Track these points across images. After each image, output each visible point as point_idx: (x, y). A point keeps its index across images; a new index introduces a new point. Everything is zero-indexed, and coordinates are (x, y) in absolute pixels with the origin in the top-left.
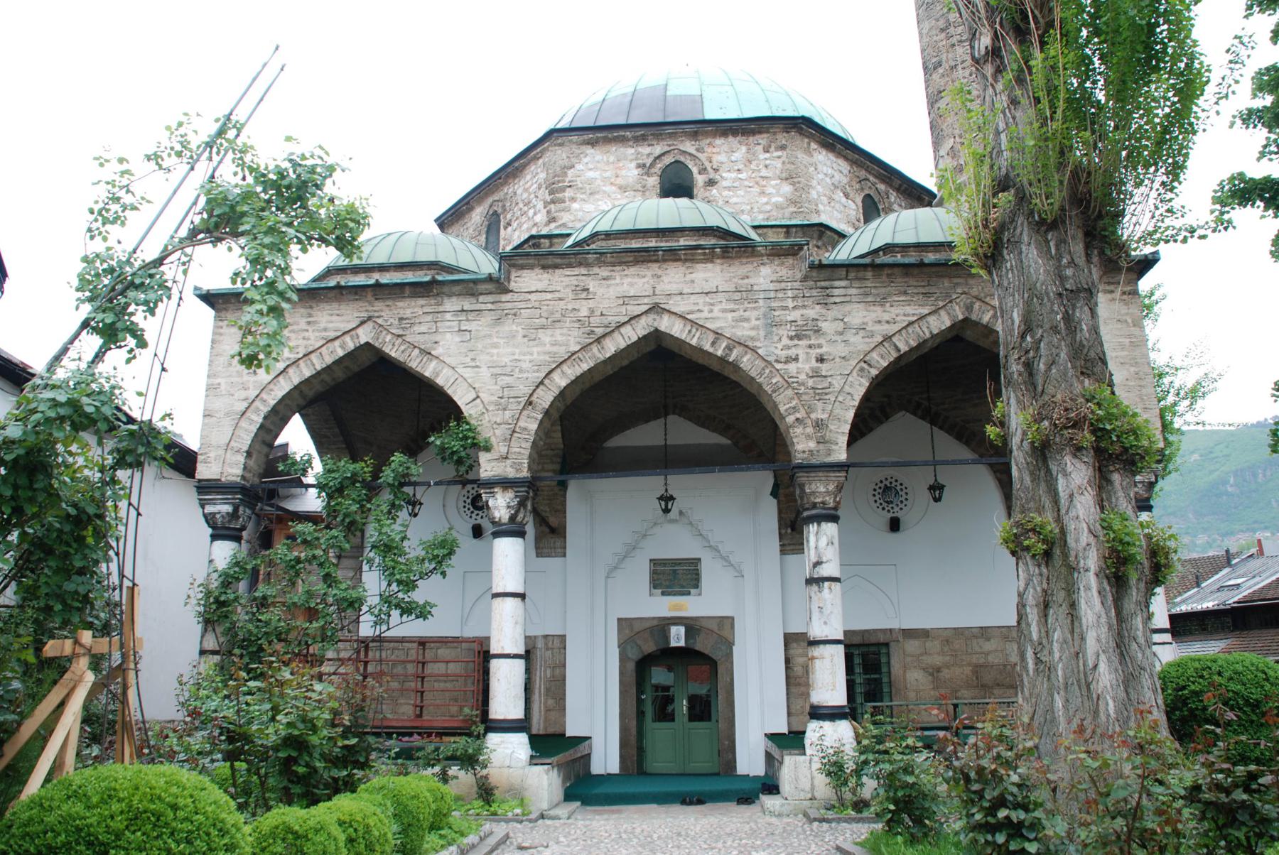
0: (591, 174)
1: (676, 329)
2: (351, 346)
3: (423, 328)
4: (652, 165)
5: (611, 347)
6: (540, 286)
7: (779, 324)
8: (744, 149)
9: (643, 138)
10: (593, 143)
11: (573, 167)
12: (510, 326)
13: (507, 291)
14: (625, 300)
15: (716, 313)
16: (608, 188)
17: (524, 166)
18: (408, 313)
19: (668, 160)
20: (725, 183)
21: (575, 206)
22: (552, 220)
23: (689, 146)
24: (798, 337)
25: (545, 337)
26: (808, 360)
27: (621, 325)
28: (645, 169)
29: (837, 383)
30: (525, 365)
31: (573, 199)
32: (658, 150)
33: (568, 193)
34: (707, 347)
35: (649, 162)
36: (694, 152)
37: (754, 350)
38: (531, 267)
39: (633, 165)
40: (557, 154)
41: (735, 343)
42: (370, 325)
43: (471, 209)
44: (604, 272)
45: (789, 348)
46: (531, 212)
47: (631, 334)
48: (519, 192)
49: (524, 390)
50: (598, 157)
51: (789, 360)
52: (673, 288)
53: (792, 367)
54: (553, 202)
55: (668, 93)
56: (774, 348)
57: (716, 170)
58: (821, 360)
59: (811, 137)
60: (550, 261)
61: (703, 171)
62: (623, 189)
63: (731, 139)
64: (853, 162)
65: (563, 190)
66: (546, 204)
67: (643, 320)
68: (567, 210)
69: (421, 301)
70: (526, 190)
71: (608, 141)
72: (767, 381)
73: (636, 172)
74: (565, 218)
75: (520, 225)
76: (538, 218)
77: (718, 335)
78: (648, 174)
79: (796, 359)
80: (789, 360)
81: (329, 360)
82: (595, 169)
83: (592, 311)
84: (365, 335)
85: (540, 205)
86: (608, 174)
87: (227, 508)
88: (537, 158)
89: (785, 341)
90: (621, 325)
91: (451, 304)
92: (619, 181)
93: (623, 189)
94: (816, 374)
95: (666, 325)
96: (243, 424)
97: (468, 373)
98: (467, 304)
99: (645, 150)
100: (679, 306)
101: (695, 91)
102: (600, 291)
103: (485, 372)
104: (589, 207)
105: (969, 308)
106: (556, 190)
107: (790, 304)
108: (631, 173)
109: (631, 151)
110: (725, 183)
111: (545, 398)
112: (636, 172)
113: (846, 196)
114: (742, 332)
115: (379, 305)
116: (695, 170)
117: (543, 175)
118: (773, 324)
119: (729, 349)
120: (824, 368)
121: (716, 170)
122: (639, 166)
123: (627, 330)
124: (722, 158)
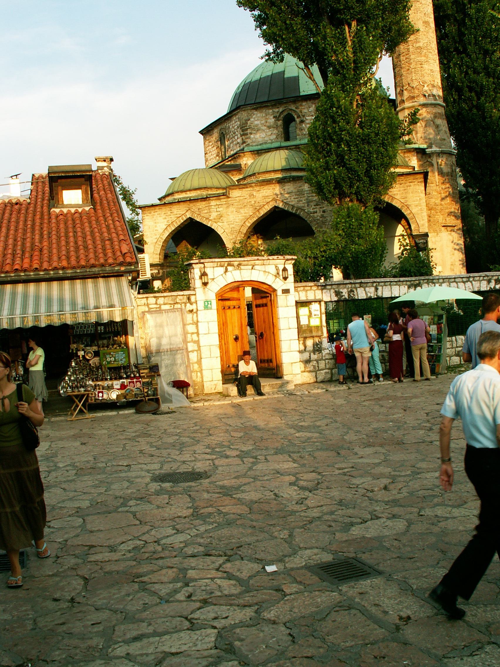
0: (256, 122)
2: (185, 219)
3: (206, 211)
4: (279, 116)
5: (263, 212)
7: (312, 201)
8: (314, 106)
9: (275, 105)
10: (256, 109)
11: (249, 120)
12: (231, 209)
13: (228, 197)
15: (292, 199)
17: (231, 117)
19: (285, 113)
20: (307, 122)
21: (252, 136)
22: (244, 142)
23: (293, 107)
24: (317, 205)
25: (242, 211)
26: (320, 212)
27: (264, 205)
28: (276, 118)
29: (329, 219)
30: (237, 221)
31: (251, 134)
32: (281, 110)
33: (249, 131)
34: (290, 210)
35: (278, 115)
36: (294, 109)
37: (304, 210)
38: (236, 189)
39: (272, 117)
40: (243, 115)
41: (298, 208)
42: (189, 211)
43: (213, 129)
44: (257, 188)
45: (313, 209)
46: (236, 137)
47: (267, 208)
48: (231, 127)
50: (259, 115)
53: (315, 215)
54: (244, 135)
55: (286, 76)
57: (304, 116)
58: (324, 212)
60: (241, 186)
61: (299, 117)
63: (308, 102)
65: (247, 130)
66: (241, 136)
67: (271, 203)
68: (249, 138)
69: (204, 203)
70: (233, 127)
71: (261, 107)
72: (309, 220)
73: (273, 120)
74: (249, 141)
75: (233, 142)
76: (239, 140)
77: (293, 206)
78: (279, 121)
79: (316, 212)
81: (179, 224)
82: (258, 120)
83: (255, 202)
84: (189, 215)
85: (239, 136)
86: (263, 122)
87: (157, 271)
88: (235, 115)
89: (313, 207)
90: (264, 205)
91: (213, 203)
92: (268, 124)
93: (269, 127)
94: (322, 216)
96: (157, 246)
98: (218, 202)
99: (277, 110)
101: (296, 75)
102: (257, 195)
106: (244, 130)
108: (272, 120)
109: (271, 111)
110: (307, 122)
112: (273, 120)
114: (301, 205)
115: (191, 205)
116: (296, 117)
117: (239, 123)
118: (309, 202)
119: (297, 210)
120: (325, 215)
121: (304, 116)
122: (274, 117)
123: (266, 207)
124: (306, 111)
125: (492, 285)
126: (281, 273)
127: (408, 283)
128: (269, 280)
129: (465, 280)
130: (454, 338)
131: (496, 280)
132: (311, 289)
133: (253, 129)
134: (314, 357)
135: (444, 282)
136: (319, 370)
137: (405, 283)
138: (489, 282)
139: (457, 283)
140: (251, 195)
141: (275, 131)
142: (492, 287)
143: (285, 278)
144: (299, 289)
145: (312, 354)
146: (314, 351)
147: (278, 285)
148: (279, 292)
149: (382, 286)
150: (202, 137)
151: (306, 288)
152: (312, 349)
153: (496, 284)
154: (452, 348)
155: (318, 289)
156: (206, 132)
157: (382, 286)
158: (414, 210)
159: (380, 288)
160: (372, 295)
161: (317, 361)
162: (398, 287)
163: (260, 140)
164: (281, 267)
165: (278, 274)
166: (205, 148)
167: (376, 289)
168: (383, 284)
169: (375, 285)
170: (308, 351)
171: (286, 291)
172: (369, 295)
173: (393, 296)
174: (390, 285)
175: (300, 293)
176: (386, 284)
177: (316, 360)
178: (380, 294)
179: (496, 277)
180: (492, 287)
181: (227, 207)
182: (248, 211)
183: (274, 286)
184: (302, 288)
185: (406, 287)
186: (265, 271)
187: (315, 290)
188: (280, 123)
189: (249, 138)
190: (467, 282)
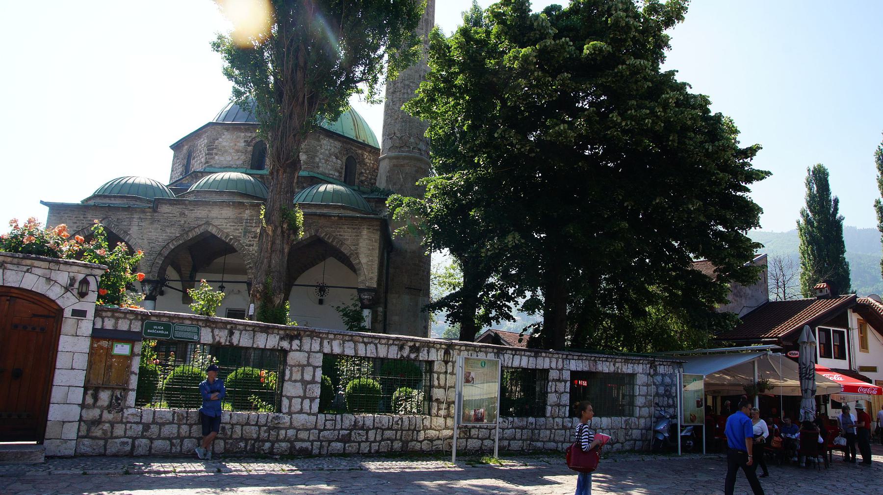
0: (224, 144)
1: (214, 231)
5: (191, 236)
6: (168, 211)
7: (250, 232)
14: (197, 219)
16: (231, 151)
18: (120, 217)
19: (258, 140)
21: (217, 157)
28: (248, 143)
31: (216, 154)
33: (215, 151)
47: (198, 231)
49: (159, 249)
50: (228, 137)
51: (250, 245)
52: (215, 215)
53: (251, 248)
56: (245, 241)
59: (320, 133)
62: (237, 151)
64: (343, 142)
65: (213, 149)
67: (203, 227)
73: (243, 144)
77: (228, 235)
80: (250, 245)
88: (205, 132)
93: (237, 151)
95: (210, 229)
97: (140, 241)
100: (216, 222)
103: (146, 241)
104: (222, 159)
105: (317, 231)
107: (254, 225)
111: (166, 253)
112: (243, 144)
113: (337, 158)
114: (237, 234)
122: (245, 141)
123: (197, 230)
125: (406, 352)
126: (77, 285)
127: (281, 332)
128: (54, 293)
129: (366, 340)
130: (339, 417)
131: (410, 347)
132: (125, 318)
133: (219, 150)
134: (107, 416)
135: (335, 339)
136: (112, 437)
137: (276, 331)
138: (401, 348)
139: (355, 342)
140: (182, 214)
141: (243, 157)
142: (405, 355)
143: (82, 295)
144: (104, 314)
145: (105, 412)
146: (110, 408)
147: (69, 303)
148: (67, 313)
149: (241, 331)
150: (172, 152)
151: (117, 315)
152: (106, 404)
153: (411, 352)
154: (334, 430)
155: (136, 319)
156: (176, 147)
157: (241, 331)
158: (364, 260)
159: (237, 334)
160: (223, 341)
161: (112, 424)
162: (264, 335)
163: (224, 162)
164: (80, 277)
165: (72, 285)
166: (173, 164)
167: (231, 333)
168: (241, 327)
169: (229, 327)
170: (99, 407)
171: (79, 314)
172: (217, 339)
173: (255, 346)
174: (253, 330)
175: (106, 320)
176: (248, 328)
177: (109, 422)
178: (235, 341)
179: (411, 344)
180: (405, 355)
181: (152, 223)
182: (175, 232)
183: (59, 302)
184: (109, 314)
185: (278, 337)
186: (49, 280)
187: (131, 320)
188: (250, 149)
189: (214, 158)
190: (370, 343)
